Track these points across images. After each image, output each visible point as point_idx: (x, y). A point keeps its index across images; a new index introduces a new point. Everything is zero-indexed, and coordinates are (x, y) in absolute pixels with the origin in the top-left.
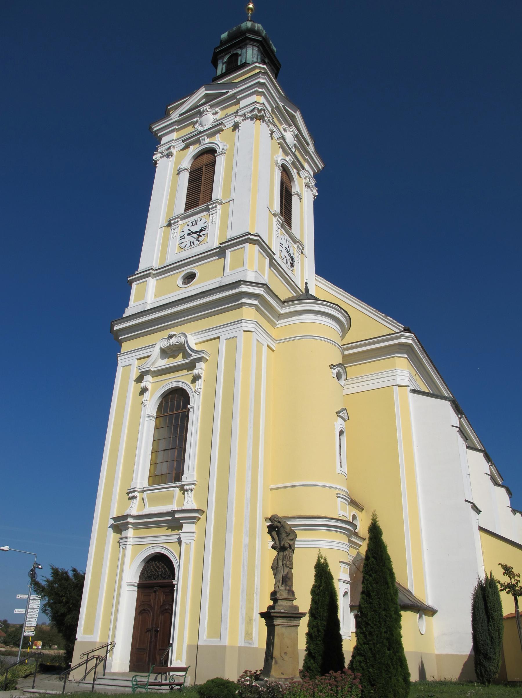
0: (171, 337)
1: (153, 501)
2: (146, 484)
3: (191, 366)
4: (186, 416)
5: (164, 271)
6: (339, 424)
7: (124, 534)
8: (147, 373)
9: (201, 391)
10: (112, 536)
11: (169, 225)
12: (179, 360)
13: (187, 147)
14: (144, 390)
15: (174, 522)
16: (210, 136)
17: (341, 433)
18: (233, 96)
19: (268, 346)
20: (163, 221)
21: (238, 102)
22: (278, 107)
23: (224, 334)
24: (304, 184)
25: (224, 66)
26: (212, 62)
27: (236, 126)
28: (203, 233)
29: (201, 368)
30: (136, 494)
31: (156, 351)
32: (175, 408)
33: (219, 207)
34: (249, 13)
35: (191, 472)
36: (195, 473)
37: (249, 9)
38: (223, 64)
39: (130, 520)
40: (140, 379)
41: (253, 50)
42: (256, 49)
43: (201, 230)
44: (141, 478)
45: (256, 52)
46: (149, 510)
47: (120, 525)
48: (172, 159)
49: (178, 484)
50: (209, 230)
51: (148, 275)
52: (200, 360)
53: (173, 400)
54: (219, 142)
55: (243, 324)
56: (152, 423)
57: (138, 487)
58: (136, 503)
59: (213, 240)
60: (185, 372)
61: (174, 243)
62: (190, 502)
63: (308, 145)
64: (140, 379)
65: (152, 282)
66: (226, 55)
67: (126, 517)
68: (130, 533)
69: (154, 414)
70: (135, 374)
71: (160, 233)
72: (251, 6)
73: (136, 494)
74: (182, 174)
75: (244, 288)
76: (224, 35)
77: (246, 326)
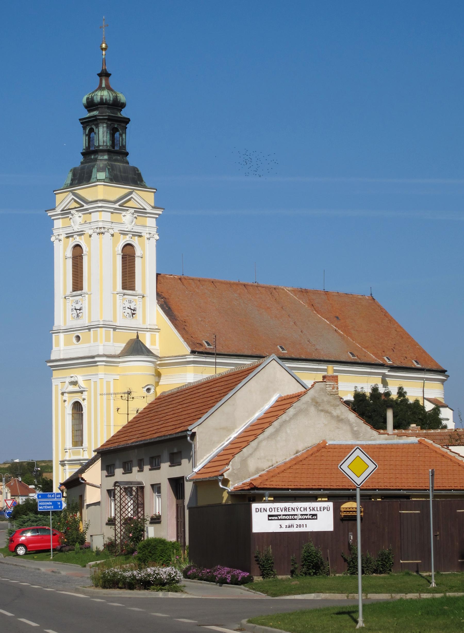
0: (72, 377)
1: (74, 454)
2: (71, 446)
3: (82, 392)
4: (82, 414)
5: (66, 331)
7: (65, 467)
8: (65, 392)
10: (60, 467)
11: (65, 298)
12: (76, 388)
13: (68, 237)
14: (65, 401)
16: (78, 235)
18: (86, 210)
21: (90, 213)
22: (116, 209)
23: (93, 379)
24: (146, 239)
27: (90, 236)
28: (81, 311)
29: (85, 395)
30: (67, 450)
31: (67, 383)
33: (87, 296)
39: (66, 462)
40: (63, 394)
41: (103, 127)
43: (80, 310)
44: (69, 444)
45: (105, 129)
47: (63, 463)
48: (62, 243)
49: (81, 447)
50: (83, 309)
51: (59, 332)
52: (84, 391)
53: (77, 405)
55: (99, 376)
57: (68, 447)
58: (68, 454)
59: (84, 321)
60: (80, 394)
61: (69, 312)
64: (63, 394)
65: (62, 336)
66: (87, 126)
67: (63, 461)
68: (67, 467)
69: (71, 412)
70: (60, 392)
71: (62, 300)
73: (67, 450)
75: (97, 359)
77: (100, 376)
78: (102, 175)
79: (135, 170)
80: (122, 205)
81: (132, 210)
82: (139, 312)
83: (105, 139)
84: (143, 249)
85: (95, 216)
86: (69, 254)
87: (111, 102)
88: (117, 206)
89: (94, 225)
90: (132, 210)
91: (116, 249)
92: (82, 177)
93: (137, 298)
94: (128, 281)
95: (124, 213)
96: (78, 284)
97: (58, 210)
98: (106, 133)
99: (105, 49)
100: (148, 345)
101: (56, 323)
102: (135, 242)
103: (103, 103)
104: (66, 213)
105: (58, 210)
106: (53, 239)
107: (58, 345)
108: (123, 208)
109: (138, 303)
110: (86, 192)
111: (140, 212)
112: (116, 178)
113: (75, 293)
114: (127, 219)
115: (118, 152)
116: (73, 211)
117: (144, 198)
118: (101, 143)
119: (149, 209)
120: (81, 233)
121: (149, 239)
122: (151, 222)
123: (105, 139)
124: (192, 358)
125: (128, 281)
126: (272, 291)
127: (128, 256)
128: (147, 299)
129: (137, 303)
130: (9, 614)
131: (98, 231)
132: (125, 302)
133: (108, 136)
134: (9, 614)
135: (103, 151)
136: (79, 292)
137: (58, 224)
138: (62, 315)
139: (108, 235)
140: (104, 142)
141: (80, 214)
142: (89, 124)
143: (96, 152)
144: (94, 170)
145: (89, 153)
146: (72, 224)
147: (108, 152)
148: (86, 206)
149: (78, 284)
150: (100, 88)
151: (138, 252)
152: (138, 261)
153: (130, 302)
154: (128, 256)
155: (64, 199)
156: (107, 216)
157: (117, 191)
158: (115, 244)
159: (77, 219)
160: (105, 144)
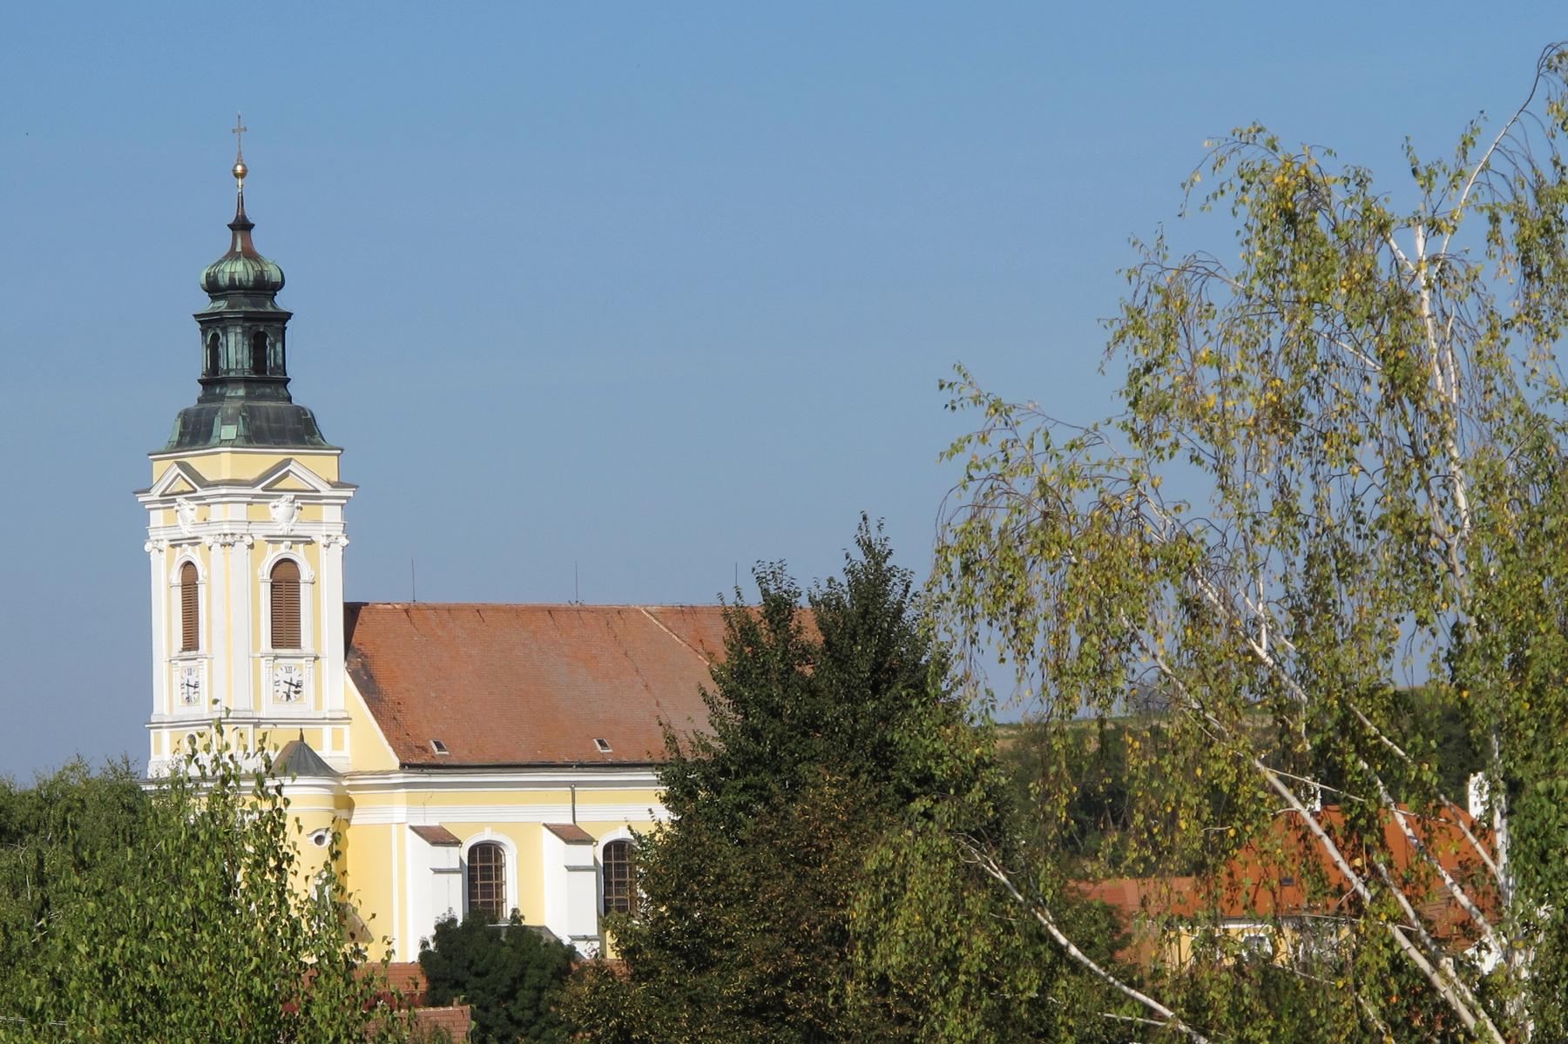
5: (173, 725)
13: (173, 546)
20: (165, 657)
22: (255, 496)
45: (240, 337)
48: (164, 555)
71: (165, 665)
78: (229, 432)
79: (300, 412)
80: (270, 485)
81: (291, 496)
82: (308, 689)
84: (316, 566)
85: (217, 512)
86: (177, 578)
88: (258, 490)
89: (216, 529)
90: (291, 496)
91: (259, 572)
92: (196, 432)
93: (303, 661)
94: (285, 630)
95: (274, 502)
96: (191, 641)
97: (155, 494)
99: (243, 175)
100: (325, 752)
101: (156, 710)
102: (299, 554)
103: (234, 287)
104: (168, 498)
105: (155, 494)
106: (148, 546)
107: (159, 751)
108: (272, 491)
109: (306, 671)
110: (201, 462)
111: (308, 496)
112: (257, 435)
113: (186, 654)
114: (280, 513)
115: (267, 375)
116: (180, 499)
117: (312, 468)
119: (325, 490)
120: (194, 541)
121: (328, 546)
122: (332, 515)
124: (399, 778)
125: (285, 630)
126: (613, 617)
127: (285, 582)
128: (325, 663)
129: (303, 671)
131: (221, 540)
132: (279, 671)
133: (246, 352)
135: (235, 381)
136: (193, 653)
137: (157, 518)
138: (166, 699)
139: (241, 547)
141: (192, 504)
142: (211, 324)
143: (224, 382)
144: (217, 421)
145: (213, 380)
146: (180, 522)
147: (247, 382)
148: (201, 492)
149: (191, 641)
150: (232, 255)
151: (305, 574)
152: (305, 592)
153: (289, 670)
154: (285, 582)
155: (165, 472)
156: (240, 512)
157: (260, 461)
158: (255, 564)
159: (188, 511)
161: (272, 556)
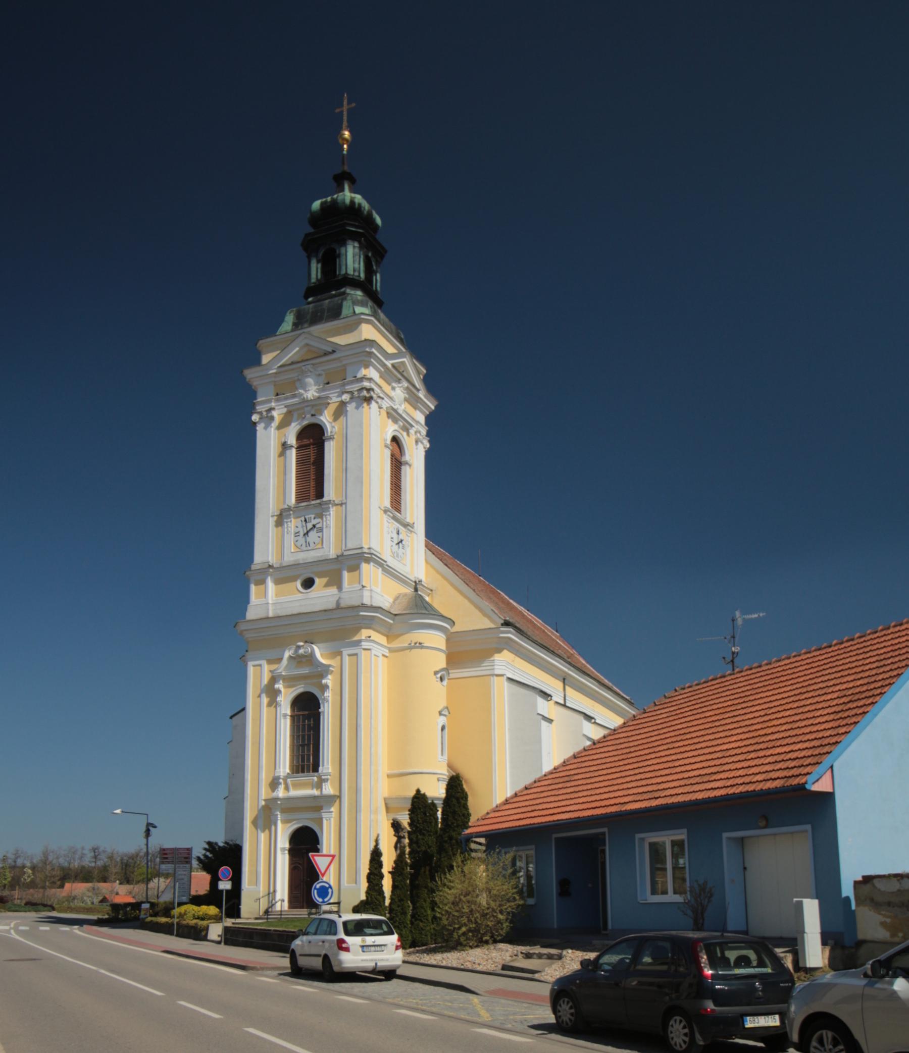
1: (296, 786)
6: (442, 720)
9: (330, 699)
15: (318, 805)
17: (443, 728)
19: (384, 655)
25: (319, 265)
26: (302, 245)
32: (307, 709)
34: (343, 149)
35: (328, 765)
36: (330, 766)
37: (345, 139)
38: (318, 262)
41: (354, 247)
42: (356, 244)
45: (357, 250)
46: (294, 793)
54: (326, 419)
55: (363, 643)
56: (288, 720)
61: (290, 540)
62: (329, 789)
63: (418, 390)
69: (289, 712)
72: (347, 134)
74: (288, 452)
76: (316, 205)
83: (357, 266)
87: (365, 212)
98: (357, 257)
106: (255, 418)
118: (350, 272)
123: (357, 266)
130: (251, 1030)
133: (362, 264)
134: (251, 1030)
140: (354, 271)
160: (357, 274)
161: (391, 429)
